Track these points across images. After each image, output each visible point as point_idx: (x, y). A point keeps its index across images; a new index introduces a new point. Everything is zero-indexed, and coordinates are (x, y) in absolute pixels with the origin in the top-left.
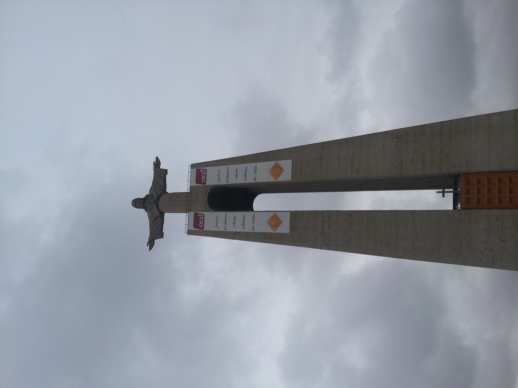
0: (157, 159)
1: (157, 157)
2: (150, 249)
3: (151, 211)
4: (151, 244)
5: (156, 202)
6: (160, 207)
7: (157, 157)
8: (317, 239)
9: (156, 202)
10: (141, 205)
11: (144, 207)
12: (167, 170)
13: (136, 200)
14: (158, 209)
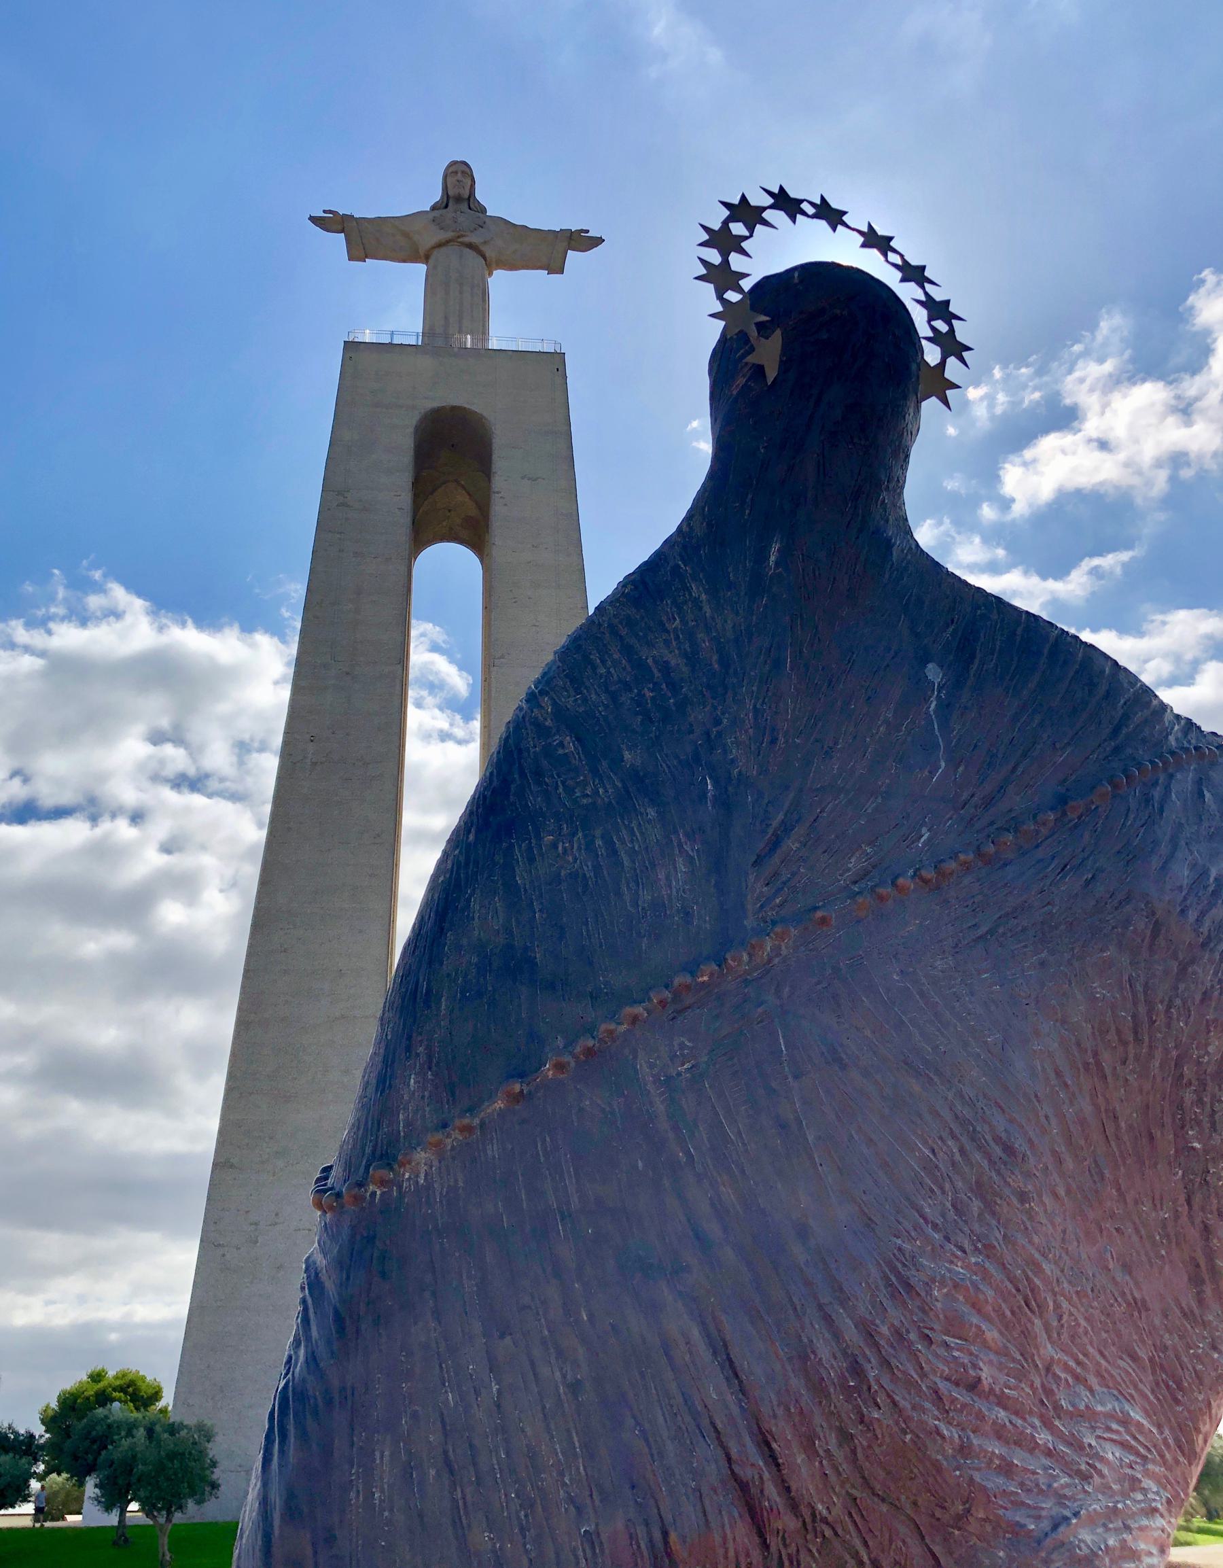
2: (314, 220)
4: (329, 222)
6: (443, 249)
8: (312, 741)
9: (459, 240)
14: (440, 245)
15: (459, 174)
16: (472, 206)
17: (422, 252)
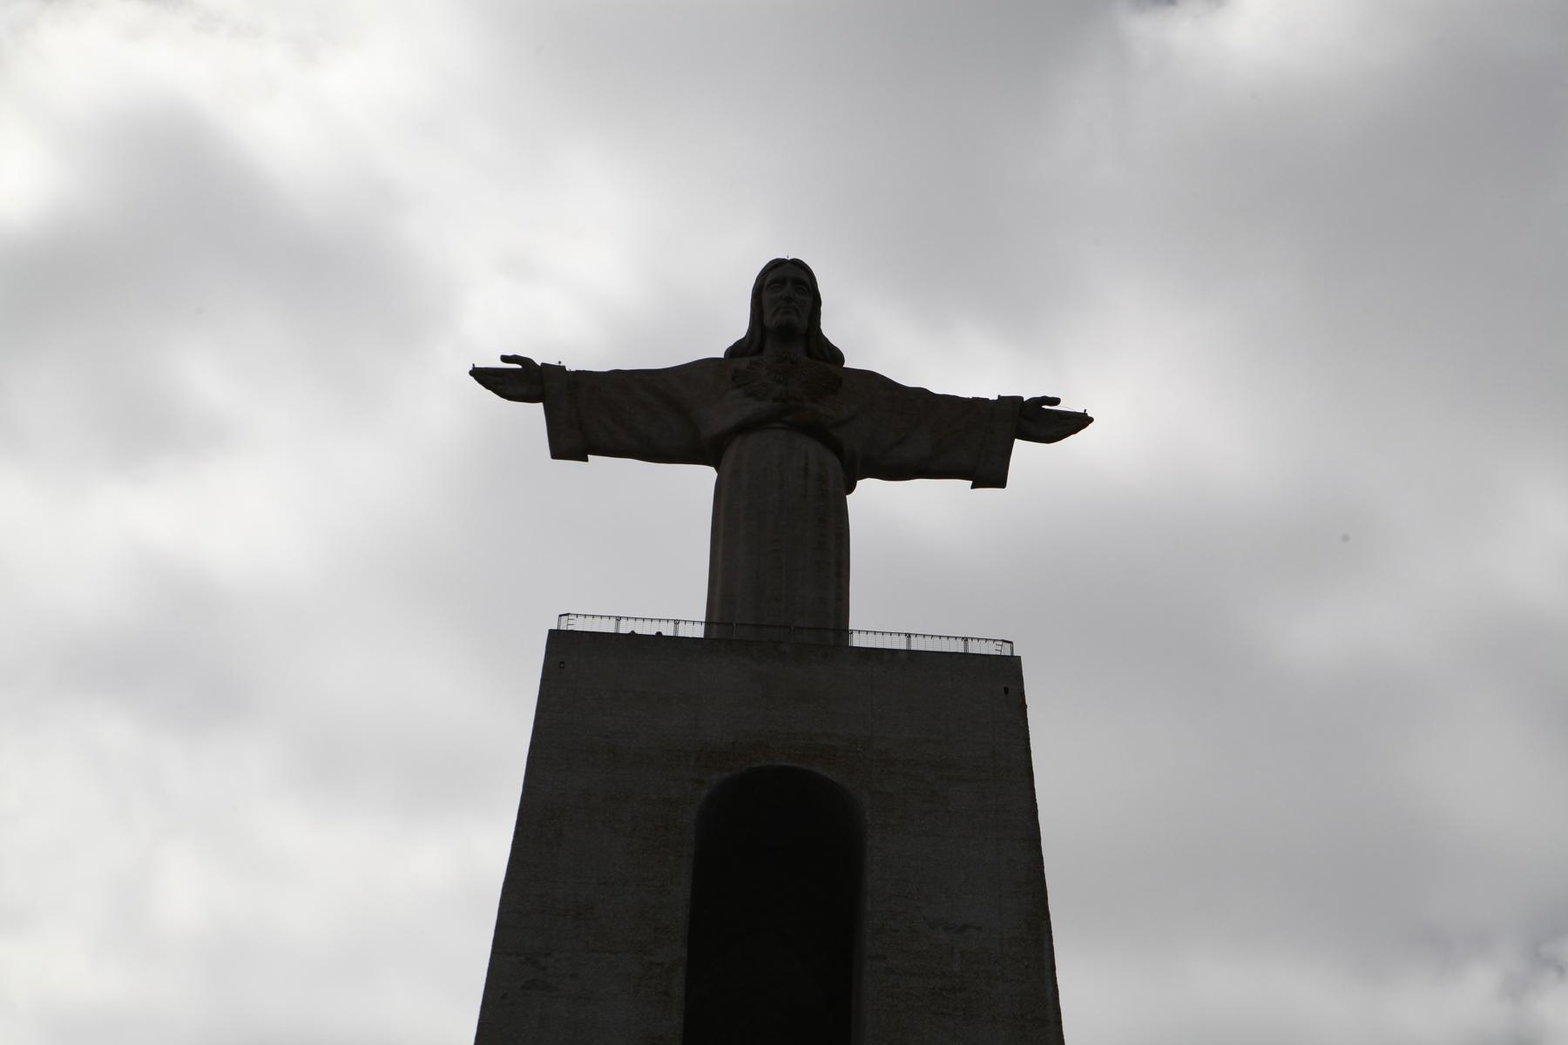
0: (1079, 421)
1: (1091, 420)
2: (483, 376)
3: (733, 378)
7: (1091, 420)
10: (770, 321)
12: (1000, 482)
13: (804, 283)
14: (744, 428)
15: (789, 285)
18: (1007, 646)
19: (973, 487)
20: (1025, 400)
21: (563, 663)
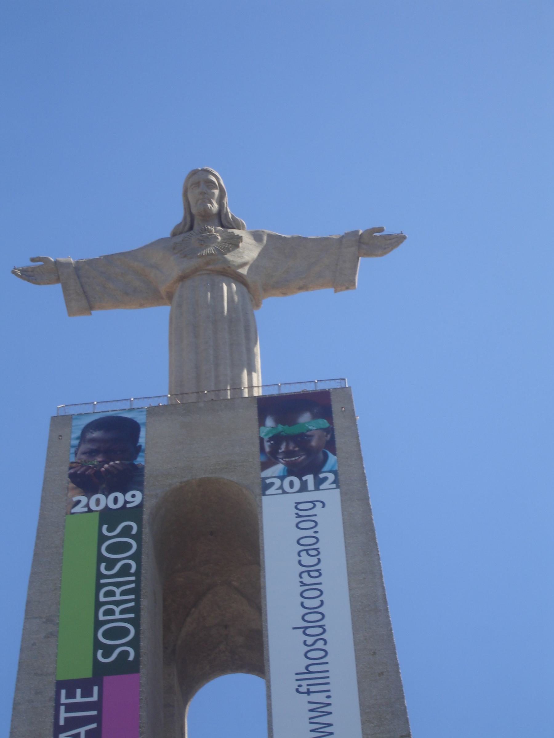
1: (404, 238)
5: (209, 267)
7: (404, 238)
9: (209, 267)
11: (189, 219)
14: (183, 278)
16: (224, 222)
17: (163, 289)
18: (343, 381)
19: (336, 291)
20: (361, 232)
21: (61, 436)
